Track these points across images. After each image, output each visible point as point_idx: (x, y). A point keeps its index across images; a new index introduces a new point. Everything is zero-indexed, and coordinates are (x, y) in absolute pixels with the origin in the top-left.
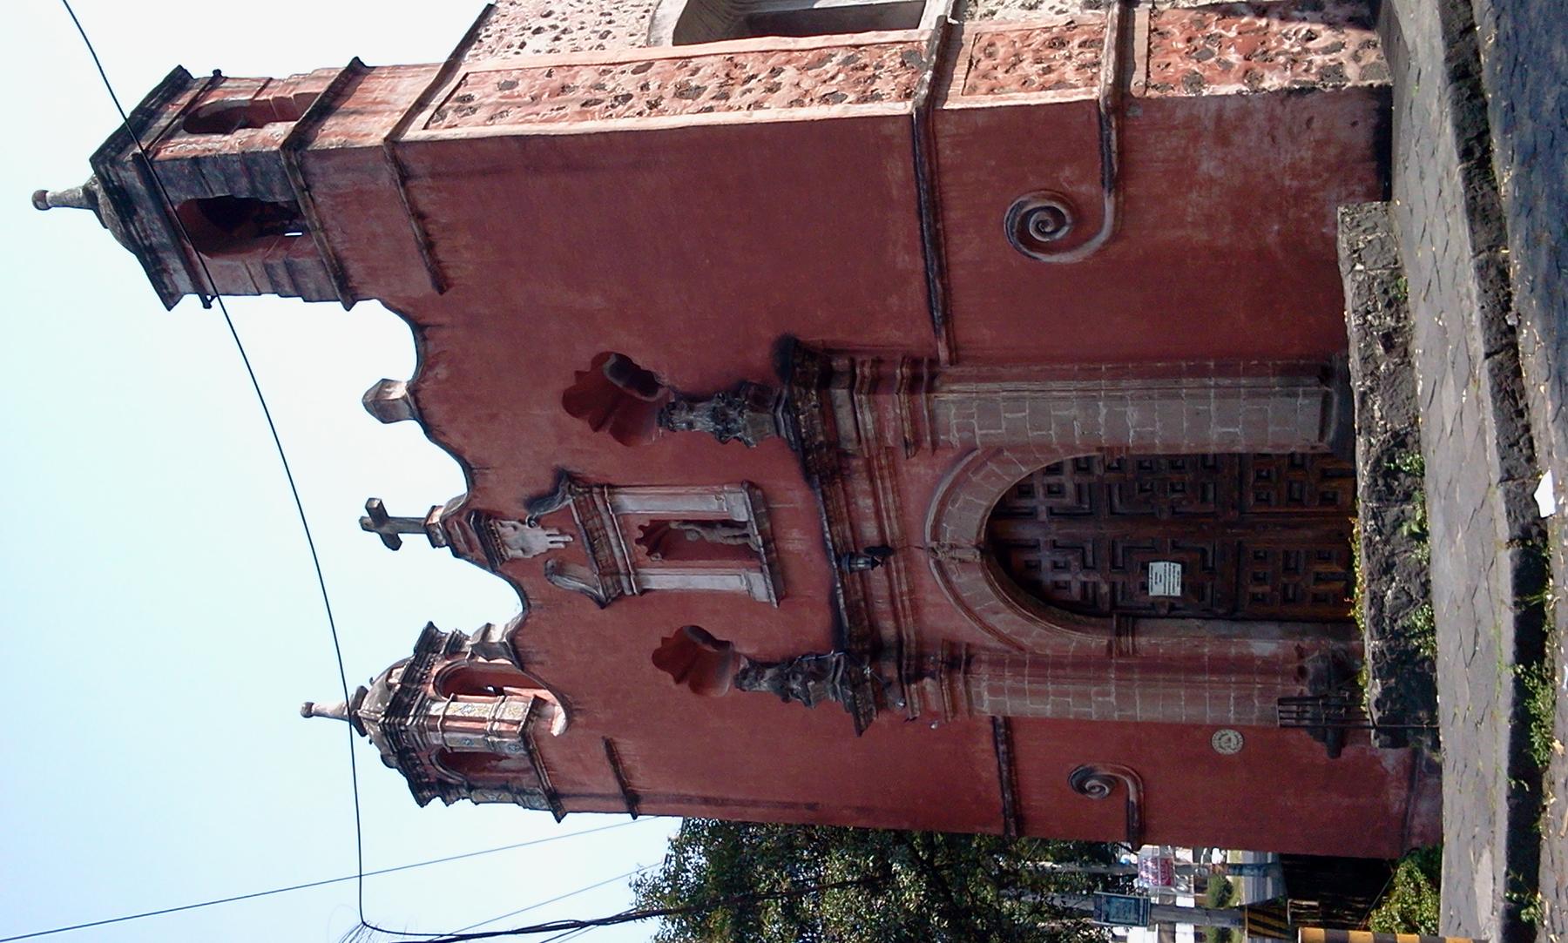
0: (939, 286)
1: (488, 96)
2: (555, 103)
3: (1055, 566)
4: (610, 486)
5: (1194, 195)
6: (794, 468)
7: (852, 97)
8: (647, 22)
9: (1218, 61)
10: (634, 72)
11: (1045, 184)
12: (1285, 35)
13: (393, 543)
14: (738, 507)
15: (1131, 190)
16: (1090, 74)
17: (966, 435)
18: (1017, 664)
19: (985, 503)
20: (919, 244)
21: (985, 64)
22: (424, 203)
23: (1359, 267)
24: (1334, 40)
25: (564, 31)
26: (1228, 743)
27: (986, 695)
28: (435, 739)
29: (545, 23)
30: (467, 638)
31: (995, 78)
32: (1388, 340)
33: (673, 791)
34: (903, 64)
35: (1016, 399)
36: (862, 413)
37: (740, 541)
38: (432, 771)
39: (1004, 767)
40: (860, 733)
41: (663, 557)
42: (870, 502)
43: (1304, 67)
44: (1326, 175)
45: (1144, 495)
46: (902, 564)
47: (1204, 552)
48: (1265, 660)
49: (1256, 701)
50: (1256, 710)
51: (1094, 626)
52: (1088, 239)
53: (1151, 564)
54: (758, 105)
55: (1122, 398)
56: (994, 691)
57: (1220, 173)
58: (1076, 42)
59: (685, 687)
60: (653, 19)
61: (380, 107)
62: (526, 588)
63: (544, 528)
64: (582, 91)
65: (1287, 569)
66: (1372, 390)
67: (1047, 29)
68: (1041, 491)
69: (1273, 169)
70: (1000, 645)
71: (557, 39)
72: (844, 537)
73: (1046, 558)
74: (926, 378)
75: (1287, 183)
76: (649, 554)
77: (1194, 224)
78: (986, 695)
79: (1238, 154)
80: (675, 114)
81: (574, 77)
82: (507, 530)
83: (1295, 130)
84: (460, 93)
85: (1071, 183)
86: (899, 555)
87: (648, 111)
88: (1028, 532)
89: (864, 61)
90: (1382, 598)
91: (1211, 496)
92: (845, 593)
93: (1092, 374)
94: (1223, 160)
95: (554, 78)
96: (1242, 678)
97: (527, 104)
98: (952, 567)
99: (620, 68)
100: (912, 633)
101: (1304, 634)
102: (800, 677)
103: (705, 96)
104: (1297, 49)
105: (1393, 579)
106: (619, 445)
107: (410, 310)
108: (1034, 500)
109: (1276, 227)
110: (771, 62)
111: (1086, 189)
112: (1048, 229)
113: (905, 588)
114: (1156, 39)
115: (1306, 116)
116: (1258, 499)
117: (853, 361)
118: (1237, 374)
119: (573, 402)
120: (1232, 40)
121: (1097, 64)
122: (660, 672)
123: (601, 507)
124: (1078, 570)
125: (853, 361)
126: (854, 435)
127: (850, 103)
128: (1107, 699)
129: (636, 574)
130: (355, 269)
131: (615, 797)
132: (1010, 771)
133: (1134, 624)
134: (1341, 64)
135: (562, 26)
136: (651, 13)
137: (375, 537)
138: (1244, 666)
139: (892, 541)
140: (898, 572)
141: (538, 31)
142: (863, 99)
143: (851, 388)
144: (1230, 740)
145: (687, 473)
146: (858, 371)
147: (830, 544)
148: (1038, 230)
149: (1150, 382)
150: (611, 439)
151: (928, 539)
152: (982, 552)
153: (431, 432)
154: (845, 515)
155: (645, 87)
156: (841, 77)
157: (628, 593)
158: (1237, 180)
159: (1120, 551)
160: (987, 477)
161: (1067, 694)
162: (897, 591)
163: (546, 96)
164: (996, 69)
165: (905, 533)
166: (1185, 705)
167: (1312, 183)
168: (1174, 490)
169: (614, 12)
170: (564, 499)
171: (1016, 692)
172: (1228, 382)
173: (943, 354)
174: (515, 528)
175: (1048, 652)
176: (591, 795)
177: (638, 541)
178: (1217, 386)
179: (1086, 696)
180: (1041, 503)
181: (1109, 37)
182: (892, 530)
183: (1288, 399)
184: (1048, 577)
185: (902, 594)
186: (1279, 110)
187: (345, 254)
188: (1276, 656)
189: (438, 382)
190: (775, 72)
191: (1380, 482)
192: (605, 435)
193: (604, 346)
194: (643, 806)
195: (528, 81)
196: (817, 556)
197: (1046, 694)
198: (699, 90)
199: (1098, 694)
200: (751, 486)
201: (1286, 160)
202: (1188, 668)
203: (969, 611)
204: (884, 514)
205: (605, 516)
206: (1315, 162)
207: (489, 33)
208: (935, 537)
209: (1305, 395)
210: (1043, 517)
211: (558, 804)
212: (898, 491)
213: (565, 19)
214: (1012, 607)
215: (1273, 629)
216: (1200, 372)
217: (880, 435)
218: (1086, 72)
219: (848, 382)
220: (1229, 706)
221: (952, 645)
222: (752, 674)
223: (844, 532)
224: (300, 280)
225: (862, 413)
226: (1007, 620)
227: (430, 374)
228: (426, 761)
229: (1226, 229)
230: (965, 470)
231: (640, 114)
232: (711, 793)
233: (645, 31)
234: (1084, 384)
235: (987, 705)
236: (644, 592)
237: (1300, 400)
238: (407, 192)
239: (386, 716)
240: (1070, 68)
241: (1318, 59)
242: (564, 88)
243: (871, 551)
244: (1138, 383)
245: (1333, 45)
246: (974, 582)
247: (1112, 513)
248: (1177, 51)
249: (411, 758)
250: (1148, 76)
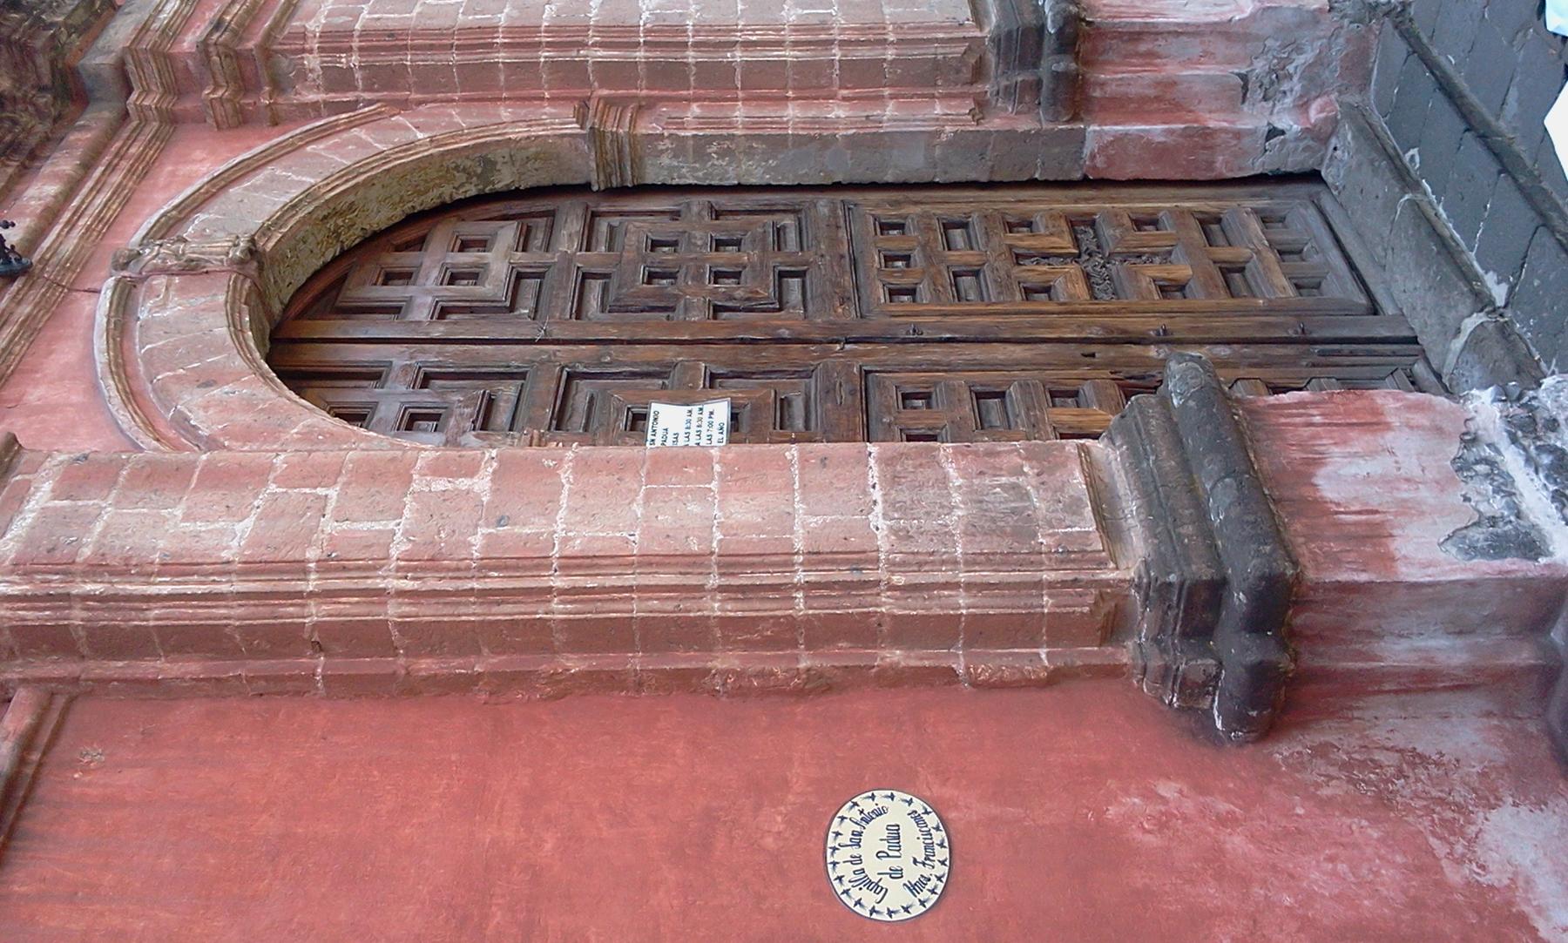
49: (951, 470)
50: (957, 498)
53: (655, 407)
68: (435, 273)
108: (411, 288)
124: (469, 424)
128: (463, 483)
139: (44, 261)
144: (895, 834)
166: (724, 491)
199: (437, 470)
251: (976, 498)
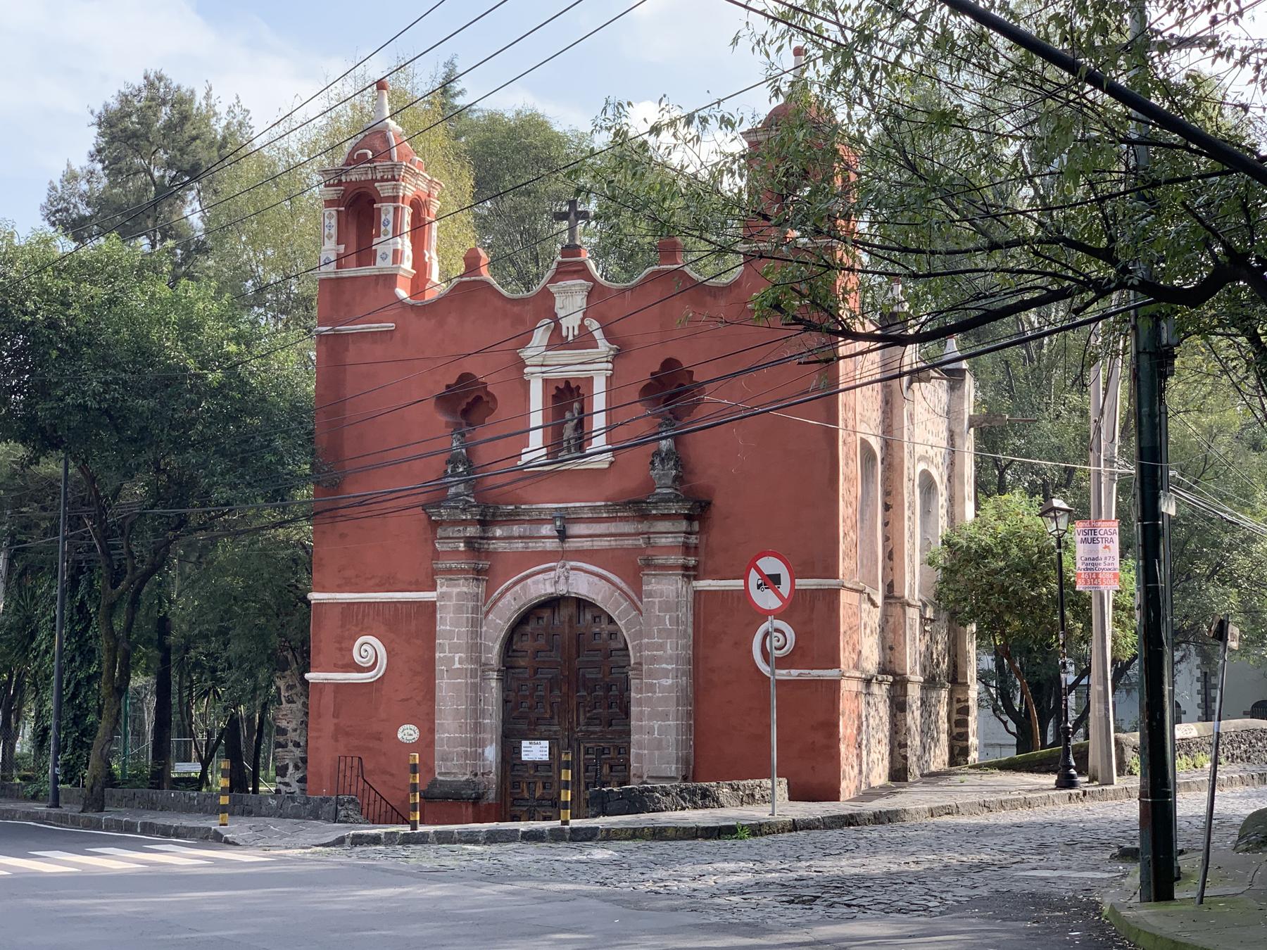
35: (678, 622)
76: (557, 388)
126: (652, 530)
128: (457, 663)
138: (480, 743)
208: (573, 569)
209: (677, 768)
220: (455, 732)
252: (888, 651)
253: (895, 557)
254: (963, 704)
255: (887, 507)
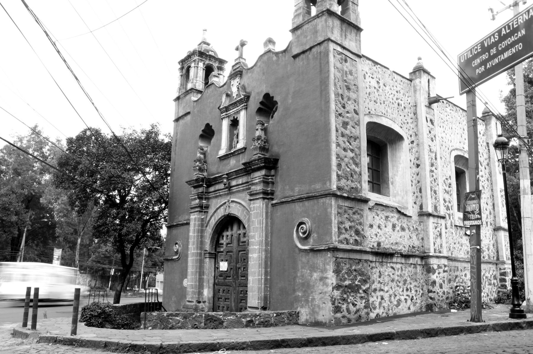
0: (290, 200)
1: (347, 67)
2: (343, 87)
3: (227, 236)
4: (246, 108)
5: (309, 271)
6: (248, 161)
7: (339, 173)
8: (381, 114)
9: (346, 278)
10: (354, 110)
11: (313, 230)
12: (355, 298)
13: (237, 49)
14: (240, 145)
15: (311, 254)
16: (343, 242)
17: (252, 209)
18: (202, 225)
19: (239, 215)
20: (301, 194)
21: (350, 212)
22: (314, 50)
23: (275, 315)
24: (352, 311)
25: (378, 90)
26: (186, 283)
27: (194, 217)
28: (193, 65)
29: (381, 84)
30: (223, 72)
31: (344, 215)
32: (251, 321)
33: (179, 131)
34: (353, 188)
36: (258, 179)
37: (234, 146)
38: (186, 64)
39: (181, 223)
40: (187, 182)
41: (231, 125)
42: (240, 183)
43: (341, 302)
44: (312, 308)
45: (243, 260)
46: (226, 192)
47: (230, 277)
48: (203, 293)
51: (212, 246)
52: (300, 242)
54: (338, 145)
55: (260, 252)
56: (195, 218)
57: (313, 278)
58: (357, 238)
59: (201, 133)
60: (381, 116)
61: (344, 37)
62: (225, 87)
63: (238, 90)
64: (348, 94)
65: (226, 299)
66: (237, 316)
67: (363, 230)
68: (244, 232)
69: (314, 293)
70: (207, 221)
71: (375, 88)
72: (233, 176)
73: (229, 233)
74: (268, 197)
75: (310, 297)
77: (302, 272)
78: (194, 217)
79: (318, 283)
80: (336, 121)
81: (354, 92)
82: (237, 80)
83: (323, 299)
84: (348, 59)
85: (313, 237)
86: (228, 192)
87: (338, 113)
88: (235, 228)
89: (355, 177)
90: (177, 316)
91: (243, 278)
92: (219, 176)
93: (267, 244)
94: (316, 280)
95: (354, 87)
96: (197, 286)
97: (343, 78)
98: (225, 206)
99: (356, 104)
100: (210, 196)
101: (209, 303)
102: (200, 165)
103: (343, 130)
104: (349, 301)
105: (183, 319)
106: (256, 110)
107: (289, 48)
109: (300, 294)
110: (356, 149)
111: (311, 240)
112: (301, 231)
113: (221, 194)
114: (357, 261)
115: (326, 302)
116: (241, 291)
117: (273, 176)
118: (265, 284)
119: (267, 96)
120: (354, 283)
121: (347, 244)
122: (204, 126)
123: (241, 106)
125: (273, 176)
126: (254, 177)
127: (337, 172)
129: (226, 117)
130: (299, 32)
131: (178, 115)
132: (180, 224)
133: (213, 258)
134: (342, 312)
135: (380, 90)
136: (384, 115)
137: (238, 44)
138: (201, 287)
139: (232, 190)
140: (225, 191)
141: (378, 82)
142: (338, 176)
143: (265, 175)
145: (250, 130)
146: (270, 177)
147: (230, 172)
148: (302, 227)
149: (264, 260)
150: (258, 107)
151: (232, 199)
152: (228, 215)
153: (261, 56)
154: (238, 176)
155: (348, 112)
156: (348, 170)
157: (222, 115)
158: (312, 283)
159: (230, 254)
160: (245, 216)
161: (194, 239)
162: (220, 191)
163: (346, 84)
164: (348, 215)
165: (234, 193)
167: (310, 304)
168: (244, 268)
169: (385, 104)
170: (243, 95)
171: (195, 224)
172: (263, 281)
173: (274, 202)
174: (238, 82)
175: (205, 234)
176: (179, 109)
177: (234, 117)
178: (262, 279)
179: (193, 244)
180: (242, 231)
181: (358, 248)
182: (234, 189)
183: (257, 298)
184: (225, 234)
185: (219, 193)
186: (327, 295)
187: (303, 29)
188: (204, 295)
189: (272, 57)
190: (352, 151)
191: (210, 317)
192: (259, 106)
193: (279, 104)
194: (176, 123)
195: (353, 79)
196: (229, 168)
197: (194, 234)
198: (346, 128)
199: (194, 247)
200: (245, 149)
201: (316, 296)
202: (201, 272)
203: (215, 212)
204: (238, 187)
205: (239, 107)
206: (315, 305)
207: (378, 68)
208: (233, 201)
209: (259, 302)
210: (239, 232)
211: (178, 99)
212: (243, 190)
213: (383, 90)
214: (216, 224)
215: (211, 295)
216: (266, 273)
217: (253, 184)
218: (344, 240)
219: (267, 174)
221: (207, 207)
222: (202, 151)
223: (234, 175)
224: (297, 17)
225: (258, 179)
226: (213, 222)
227: (274, 55)
228: (188, 63)
229: (300, 281)
230: (247, 209)
231: (337, 111)
232: (178, 142)
233: (377, 114)
234: (264, 242)
235: (193, 217)
236: (222, 119)
237: (257, 301)
238: (316, 45)
239: (198, 51)
240: (347, 236)
241: (344, 307)
242: (348, 89)
243: (229, 183)
244: (264, 257)
245: (350, 311)
246: (221, 213)
247: (239, 251)
248: (351, 267)
249: (188, 59)
250: (341, 258)
251: (190, 291)
252: (421, 241)
253: (423, 191)
254: (503, 271)
255: (418, 166)
